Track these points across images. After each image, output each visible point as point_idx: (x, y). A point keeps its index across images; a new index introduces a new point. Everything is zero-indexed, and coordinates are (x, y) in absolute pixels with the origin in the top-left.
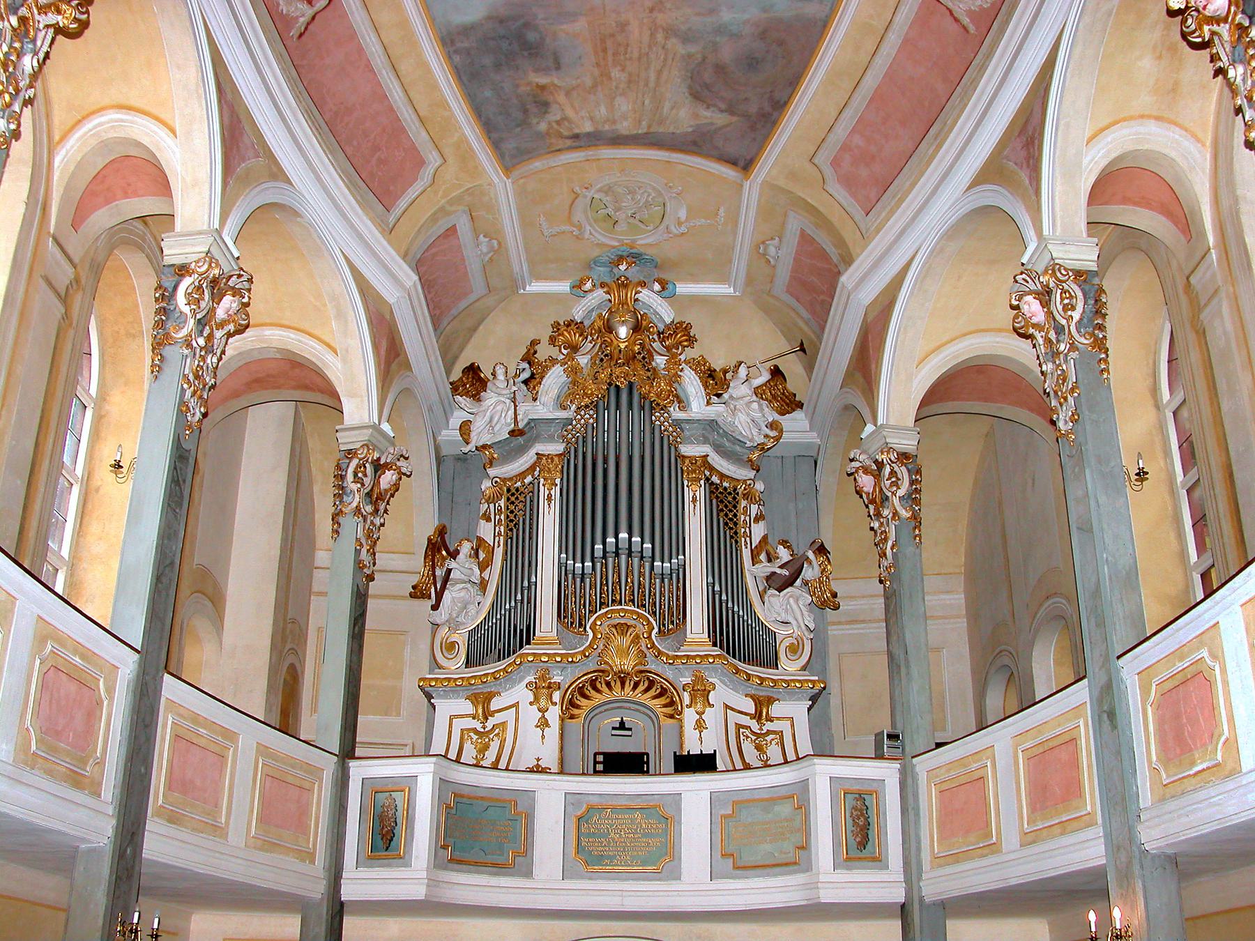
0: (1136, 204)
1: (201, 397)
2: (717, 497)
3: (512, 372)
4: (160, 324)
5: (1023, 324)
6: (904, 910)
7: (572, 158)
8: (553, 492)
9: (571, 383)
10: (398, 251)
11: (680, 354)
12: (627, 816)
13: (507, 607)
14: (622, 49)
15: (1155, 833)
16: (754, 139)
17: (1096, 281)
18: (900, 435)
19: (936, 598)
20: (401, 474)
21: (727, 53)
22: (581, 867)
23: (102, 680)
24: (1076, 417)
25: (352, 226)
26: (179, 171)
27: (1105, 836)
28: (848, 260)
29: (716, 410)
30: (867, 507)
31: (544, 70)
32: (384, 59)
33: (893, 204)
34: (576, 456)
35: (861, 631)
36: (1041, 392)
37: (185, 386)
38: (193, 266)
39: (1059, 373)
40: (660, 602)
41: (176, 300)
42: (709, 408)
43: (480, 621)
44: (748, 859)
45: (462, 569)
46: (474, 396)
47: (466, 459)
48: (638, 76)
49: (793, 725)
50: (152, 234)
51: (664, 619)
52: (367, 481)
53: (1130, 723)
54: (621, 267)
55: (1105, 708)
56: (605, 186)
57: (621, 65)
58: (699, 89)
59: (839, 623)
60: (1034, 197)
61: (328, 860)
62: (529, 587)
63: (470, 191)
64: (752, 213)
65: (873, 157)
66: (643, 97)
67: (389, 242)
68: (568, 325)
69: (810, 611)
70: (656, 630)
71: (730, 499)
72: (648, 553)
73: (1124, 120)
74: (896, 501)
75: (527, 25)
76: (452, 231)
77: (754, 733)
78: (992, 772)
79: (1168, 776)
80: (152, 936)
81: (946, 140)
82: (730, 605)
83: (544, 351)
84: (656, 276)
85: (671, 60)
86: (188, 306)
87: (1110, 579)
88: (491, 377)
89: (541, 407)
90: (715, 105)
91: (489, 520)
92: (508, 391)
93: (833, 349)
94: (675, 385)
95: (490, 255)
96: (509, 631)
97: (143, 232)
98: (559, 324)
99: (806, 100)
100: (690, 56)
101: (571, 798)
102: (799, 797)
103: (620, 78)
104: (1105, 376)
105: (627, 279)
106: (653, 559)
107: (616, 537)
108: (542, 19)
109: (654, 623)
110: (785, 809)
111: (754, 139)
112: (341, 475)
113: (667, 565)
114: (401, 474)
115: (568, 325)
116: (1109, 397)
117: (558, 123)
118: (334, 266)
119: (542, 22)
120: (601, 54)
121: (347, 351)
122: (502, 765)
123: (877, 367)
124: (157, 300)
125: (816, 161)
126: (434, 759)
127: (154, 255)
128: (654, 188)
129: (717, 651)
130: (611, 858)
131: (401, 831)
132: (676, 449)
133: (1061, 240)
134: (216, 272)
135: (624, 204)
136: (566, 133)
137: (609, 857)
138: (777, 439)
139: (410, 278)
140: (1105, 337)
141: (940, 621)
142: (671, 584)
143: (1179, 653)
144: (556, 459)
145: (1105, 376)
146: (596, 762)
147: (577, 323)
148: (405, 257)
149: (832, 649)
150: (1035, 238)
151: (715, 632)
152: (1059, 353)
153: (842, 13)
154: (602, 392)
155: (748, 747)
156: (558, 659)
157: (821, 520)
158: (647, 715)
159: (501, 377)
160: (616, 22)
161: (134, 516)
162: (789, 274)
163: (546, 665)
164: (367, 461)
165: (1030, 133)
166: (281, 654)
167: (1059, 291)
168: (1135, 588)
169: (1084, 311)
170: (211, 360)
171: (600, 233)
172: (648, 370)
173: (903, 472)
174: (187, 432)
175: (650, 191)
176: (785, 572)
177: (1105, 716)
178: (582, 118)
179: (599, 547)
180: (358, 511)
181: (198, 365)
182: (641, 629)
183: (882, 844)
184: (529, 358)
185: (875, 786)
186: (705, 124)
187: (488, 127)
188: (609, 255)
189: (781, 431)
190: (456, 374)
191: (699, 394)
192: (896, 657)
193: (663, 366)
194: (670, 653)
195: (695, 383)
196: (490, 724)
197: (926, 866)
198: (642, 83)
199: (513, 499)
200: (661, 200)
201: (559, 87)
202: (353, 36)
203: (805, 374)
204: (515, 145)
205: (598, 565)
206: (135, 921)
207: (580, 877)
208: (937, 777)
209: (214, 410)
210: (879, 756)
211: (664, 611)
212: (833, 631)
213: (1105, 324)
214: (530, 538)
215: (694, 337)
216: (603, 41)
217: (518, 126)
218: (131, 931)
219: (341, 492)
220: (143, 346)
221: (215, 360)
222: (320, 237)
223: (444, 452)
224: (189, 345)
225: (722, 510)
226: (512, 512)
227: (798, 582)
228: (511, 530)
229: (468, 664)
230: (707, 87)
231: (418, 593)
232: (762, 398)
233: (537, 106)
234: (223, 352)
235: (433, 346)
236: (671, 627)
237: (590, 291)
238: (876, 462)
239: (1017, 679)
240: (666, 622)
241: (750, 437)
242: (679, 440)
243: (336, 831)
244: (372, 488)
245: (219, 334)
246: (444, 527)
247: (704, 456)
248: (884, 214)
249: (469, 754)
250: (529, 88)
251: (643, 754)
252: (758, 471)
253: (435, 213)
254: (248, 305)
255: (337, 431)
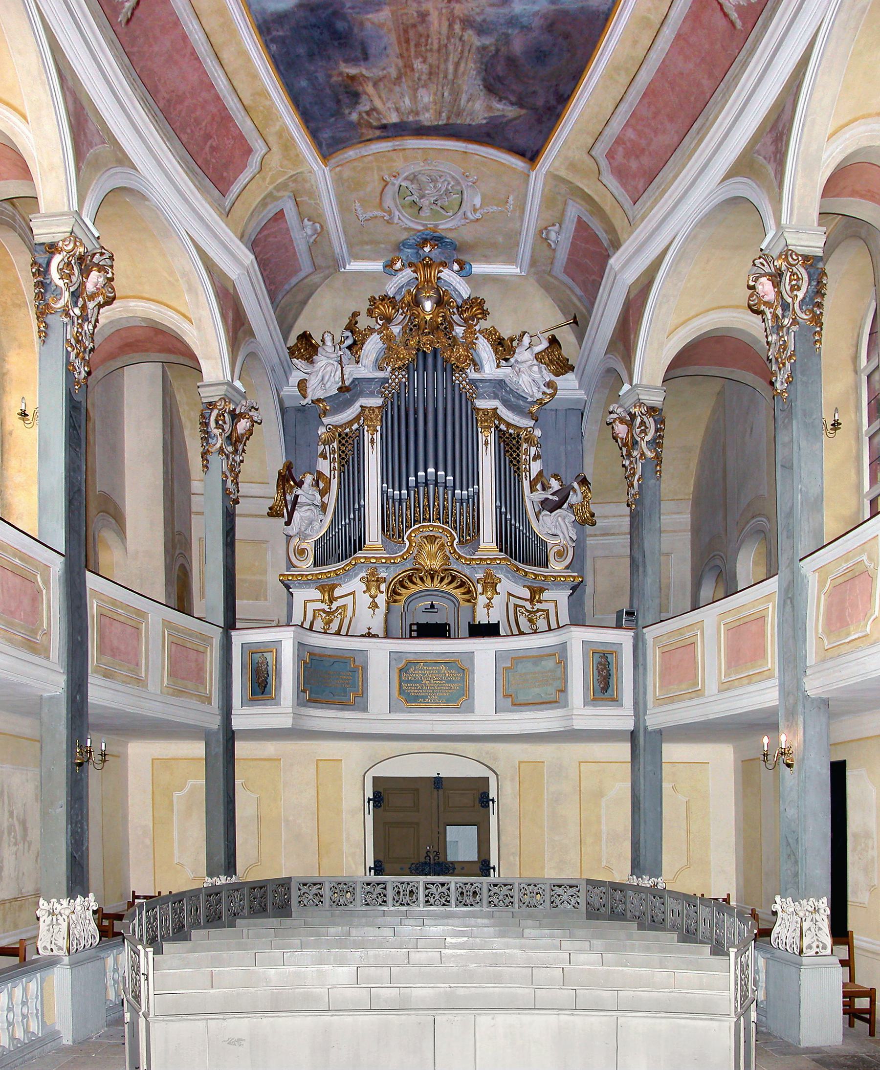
0: (862, 196)
1: (83, 358)
2: (504, 441)
3: (338, 339)
4: (40, 296)
5: (756, 301)
6: (633, 736)
7: (381, 148)
8: (375, 437)
9: (386, 348)
10: (235, 233)
11: (475, 325)
12: (435, 668)
13: (343, 523)
14: (423, 40)
15: (816, 683)
16: (541, 132)
17: (820, 265)
18: (649, 393)
19: (669, 517)
20: (253, 422)
21: (518, 46)
22: (403, 704)
23: (39, 576)
24: (791, 379)
25: (194, 210)
26: (36, 157)
27: (780, 685)
28: (616, 244)
29: (504, 372)
30: (621, 449)
31: (353, 60)
32: (207, 46)
33: (657, 194)
34: (392, 409)
35: (611, 541)
36: (765, 360)
37: (69, 349)
38: (60, 244)
39: (781, 343)
40: (460, 520)
41: (50, 274)
42: (498, 370)
43: (322, 534)
44: (522, 698)
45: (306, 495)
46: (307, 359)
47: (305, 411)
48: (438, 67)
49: (556, 606)
50: (20, 215)
51: (463, 532)
52: (226, 427)
53: (807, 606)
54: (425, 249)
55: (790, 596)
56: (410, 175)
57: (422, 57)
58: (492, 81)
59: (595, 535)
60: (777, 189)
61: (221, 703)
62: (359, 509)
63: (294, 178)
64: (537, 202)
65: (643, 151)
66: (443, 88)
67: (227, 225)
68: (383, 300)
69: (574, 527)
70: (457, 540)
71: (514, 442)
72: (450, 484)
73: (863, 117)
74: (644, 445)
75: (336, 14)
76: (280, 215)
77: (527, 611)
78: (701, 639)
79: (829, 644)
80: (101, 755)
81: (707, 134)
82: (513, 522)
83: (364, 322)
84: (455, 257)
85: (467, 52)
86: (61, 280)
87: (802, 504)
88: (321, 343)
89: (363, 368)
90: (506, 98)
91: (325, 458)
92: (335, 355)
93: (600, 322)
94: (471, 351)
95: (314, 237)
96: (346, 541)
97: (13, 213)
98: (375, 299)
99: (586, 95)
100: (484, 48)
101: (394, 656)
102: (560, 654)
103: (422, 69)
104: (817, 346)
105: (431, 259)
106: (454, 489)
107: (426, 471)
108: (350, 8)
109: (455, 535)
110: (550, 664)
111: (541, 132)
112: (205, 422)
113: (465, 492)
114: (253, 422)
115: (383, 300)
116: (819, 364)
117: (368, 113)
118: (181, 245)
119: (349, 11)
120: (404, 45)
121: (200, 320)
122: (343, 632)
123: (635, 337)
124: (34, 274)
125: (593, 153)
126: (293, 628)
127: (25, 234)
128: (453, 177)
129: (502, 555)
130: (424, 698)
131: (272, 680)
132: (472, 403)
133: (795, 229)
134: (81, 250)
135: (427, 192)
136: (375, 124)
137: (422, 697)
138: (553, 395)
139: (248, 258)
140: (821, 313)
141: (671, 534)
142: (468, 506)
143: (846, 557)
144: (377, 410)
145: (817, 346)
146: (411, 631)
147: (390, 298)
148: (241, 238)
149: (588, 553)
150: (774, 227)
151: (502, 541)
152: (782, 327)
153: (623, 6)
154: (412, 356)
155: (523, 621)
156: (384, 561)
157: (585, 459)
158: (451, 600)
159: (329, 343)
160: (417, 12)
161: (44, 454)
162: (567, 256)
163: (374, 565)
164: (225, 411)
165: (780, 129)
166: (173, 557)
167: (789, 274)
168: (820, 511)
169: (807, 292)
170: (86, 327)
171: (408, 219)
172: (449, 338)
173: (650, 422)
174: (77, 387)
175: (450, 180)
176: (556, 498)
177: (789, 602)
178: (389, 109)
179: (412, 479)
180: (221, 451)
181: (77, 332)
182: (446, 539)
183: (619, 689)
184: (351, 327)
185: (614, 648)
186: (497, 116)
187: (307, 117)
188: (415, 238)
189: (556, 389)
190: (292, 340)
191: (491, 358)
192: (637, 559)
193: (461, 335)
194: (468, 557)
195: (487, 349)
196: (335, 605)
197: (650, 705)
198: (441, 76)
199: (344, 442)
200: (459, 188)
201: (367, 78)
202: (177, 23)
203: (577, 343)
204: (331, 135)
205: (412, 492)
206: (89, 745)
207: (403, 711)
208: (661, 642)
209: (96, 369)
210: (619, 626)
211: (463, 527)
212: (590, 541)
213: (824, 303)
214: (359, 472)
215: (487, 311)
216: (406, 31)
217: (332, 116)
218: (86, 752)
219: (206, 436)
220: (29, 315)
221: (91, 327)
222: (166, 219)
223: (287, 404)
224: (67, 314)
225: (508, 451)
226: (343, 452)
227: (565, 506)
228: (343, 466)
229: (316, 564)
230: (500, 79)
231: (274, 513)
232: (541, 362)
233: (348, 97)
234: (97, 321)
235: (271, 317)
236: (468, 538)
237: (400, 270)
238: (630, 414)
239: (724, 575)
240: (464, 535)
241: (531, 393)
242: (474, 396)
243: (225, 681)
244: (231, 432)
245: (91, 305)
246: (291, 463)
247: (494, 409)
248: (649, 203)
249: (319, 625)
250: (340, 79)
251: (446, 624)
252: (536, 421)
253: (264, 199)
254: (112, 279)
255: (198, 387)
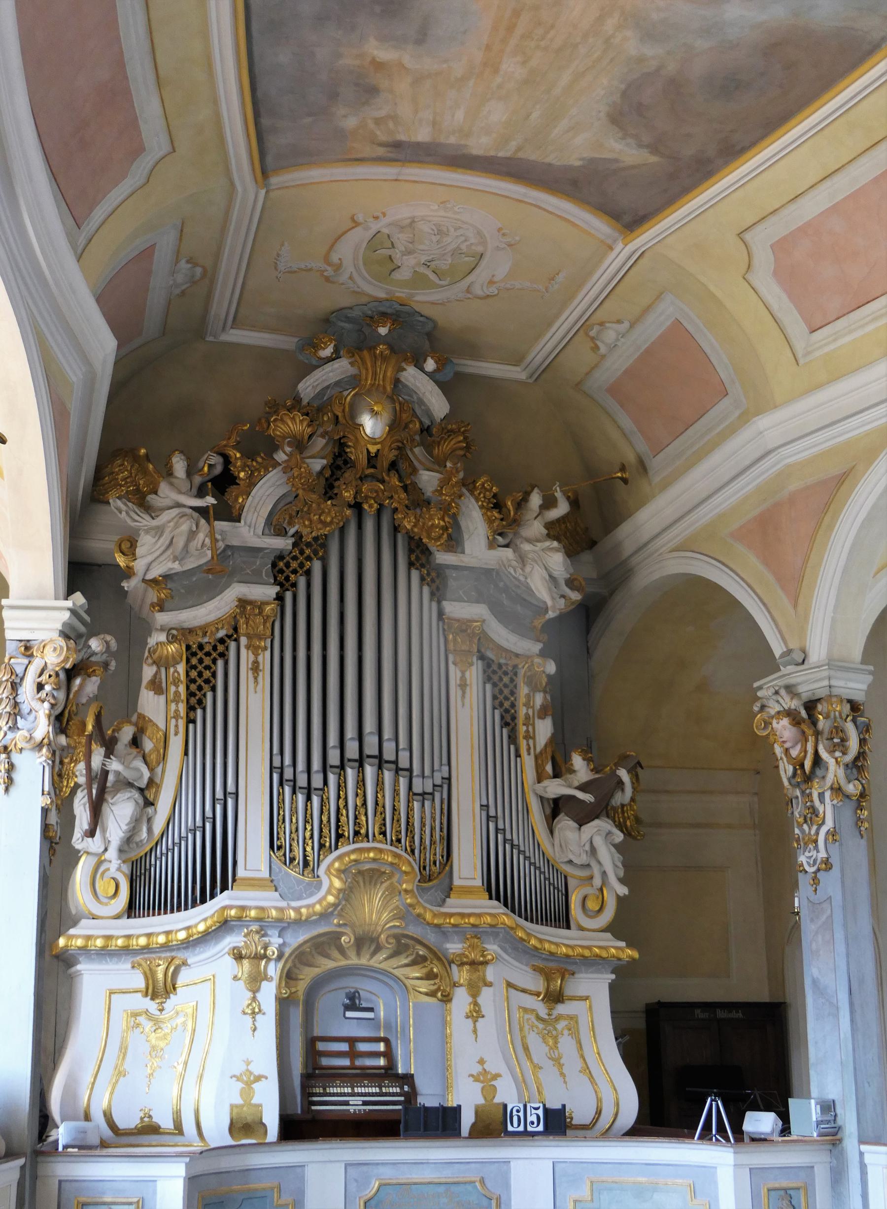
171: (364, 278)
216: (517, 13)
